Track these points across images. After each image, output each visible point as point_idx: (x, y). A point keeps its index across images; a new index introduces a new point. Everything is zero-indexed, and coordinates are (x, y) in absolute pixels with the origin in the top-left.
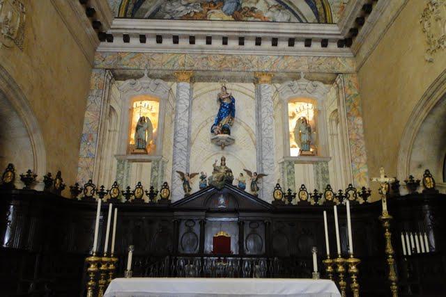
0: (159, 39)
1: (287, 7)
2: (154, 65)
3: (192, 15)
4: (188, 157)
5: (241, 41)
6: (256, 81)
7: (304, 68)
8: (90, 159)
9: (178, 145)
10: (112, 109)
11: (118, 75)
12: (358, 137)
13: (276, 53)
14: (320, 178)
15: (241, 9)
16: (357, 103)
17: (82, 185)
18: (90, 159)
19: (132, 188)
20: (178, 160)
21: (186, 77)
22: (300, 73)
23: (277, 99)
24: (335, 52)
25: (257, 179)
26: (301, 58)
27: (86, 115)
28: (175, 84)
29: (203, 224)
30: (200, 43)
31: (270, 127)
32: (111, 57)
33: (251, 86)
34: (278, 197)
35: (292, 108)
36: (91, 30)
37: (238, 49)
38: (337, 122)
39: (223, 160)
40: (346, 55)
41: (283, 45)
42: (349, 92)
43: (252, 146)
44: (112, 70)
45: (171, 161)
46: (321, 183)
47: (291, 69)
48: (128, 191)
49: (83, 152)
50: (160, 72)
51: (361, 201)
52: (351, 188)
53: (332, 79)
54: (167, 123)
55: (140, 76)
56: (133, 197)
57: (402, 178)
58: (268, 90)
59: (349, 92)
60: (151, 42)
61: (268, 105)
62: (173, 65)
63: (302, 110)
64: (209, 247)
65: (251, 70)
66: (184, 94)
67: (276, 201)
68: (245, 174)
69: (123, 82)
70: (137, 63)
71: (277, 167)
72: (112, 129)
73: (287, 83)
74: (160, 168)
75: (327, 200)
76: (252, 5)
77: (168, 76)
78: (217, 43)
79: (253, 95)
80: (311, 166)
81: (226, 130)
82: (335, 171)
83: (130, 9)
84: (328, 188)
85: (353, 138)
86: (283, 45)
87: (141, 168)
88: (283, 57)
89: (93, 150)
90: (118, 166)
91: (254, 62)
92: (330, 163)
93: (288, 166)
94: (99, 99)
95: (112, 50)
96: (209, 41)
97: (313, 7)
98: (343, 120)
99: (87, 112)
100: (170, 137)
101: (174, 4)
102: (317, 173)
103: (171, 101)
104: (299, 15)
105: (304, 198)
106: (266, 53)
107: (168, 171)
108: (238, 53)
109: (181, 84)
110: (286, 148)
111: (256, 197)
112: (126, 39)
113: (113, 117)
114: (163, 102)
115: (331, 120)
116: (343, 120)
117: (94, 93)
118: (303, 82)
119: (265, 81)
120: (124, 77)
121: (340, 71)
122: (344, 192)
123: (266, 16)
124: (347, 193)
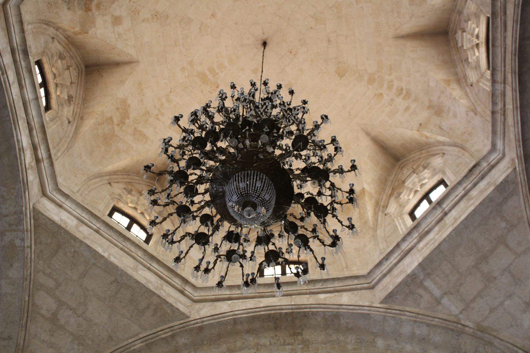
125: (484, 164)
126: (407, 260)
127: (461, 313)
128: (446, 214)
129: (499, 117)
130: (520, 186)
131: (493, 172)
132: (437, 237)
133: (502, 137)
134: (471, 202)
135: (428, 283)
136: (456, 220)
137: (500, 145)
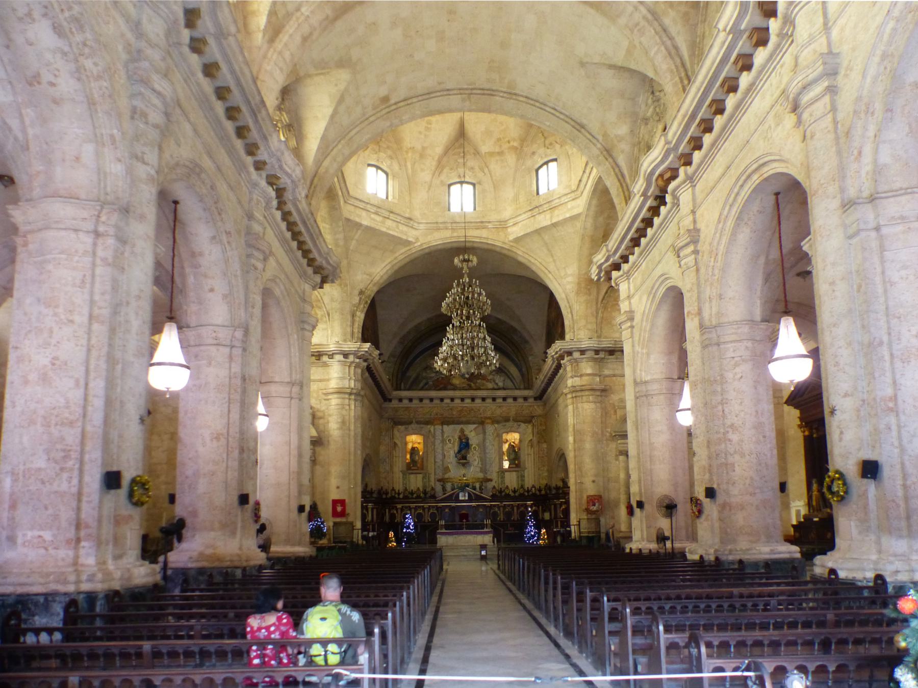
0: (421, 400)
6: (482, 423)
7: (513, 413)
11: (397, 422)
21: (439, 422)
26: (511, 408)
30: (447, 401)
44: (392, 419)
53: (529, 420)
55: (411, 423)
58: (490, 429)
60: (415, 402)
65: (479, 416)
78: (457, 401)
81: (464, 458)
88: (500, 407)
96: (452, 400)
108: (471, 405)
109: (436, 427)
112: (400, 400)
118: (511, 423)
120: (402, 424)
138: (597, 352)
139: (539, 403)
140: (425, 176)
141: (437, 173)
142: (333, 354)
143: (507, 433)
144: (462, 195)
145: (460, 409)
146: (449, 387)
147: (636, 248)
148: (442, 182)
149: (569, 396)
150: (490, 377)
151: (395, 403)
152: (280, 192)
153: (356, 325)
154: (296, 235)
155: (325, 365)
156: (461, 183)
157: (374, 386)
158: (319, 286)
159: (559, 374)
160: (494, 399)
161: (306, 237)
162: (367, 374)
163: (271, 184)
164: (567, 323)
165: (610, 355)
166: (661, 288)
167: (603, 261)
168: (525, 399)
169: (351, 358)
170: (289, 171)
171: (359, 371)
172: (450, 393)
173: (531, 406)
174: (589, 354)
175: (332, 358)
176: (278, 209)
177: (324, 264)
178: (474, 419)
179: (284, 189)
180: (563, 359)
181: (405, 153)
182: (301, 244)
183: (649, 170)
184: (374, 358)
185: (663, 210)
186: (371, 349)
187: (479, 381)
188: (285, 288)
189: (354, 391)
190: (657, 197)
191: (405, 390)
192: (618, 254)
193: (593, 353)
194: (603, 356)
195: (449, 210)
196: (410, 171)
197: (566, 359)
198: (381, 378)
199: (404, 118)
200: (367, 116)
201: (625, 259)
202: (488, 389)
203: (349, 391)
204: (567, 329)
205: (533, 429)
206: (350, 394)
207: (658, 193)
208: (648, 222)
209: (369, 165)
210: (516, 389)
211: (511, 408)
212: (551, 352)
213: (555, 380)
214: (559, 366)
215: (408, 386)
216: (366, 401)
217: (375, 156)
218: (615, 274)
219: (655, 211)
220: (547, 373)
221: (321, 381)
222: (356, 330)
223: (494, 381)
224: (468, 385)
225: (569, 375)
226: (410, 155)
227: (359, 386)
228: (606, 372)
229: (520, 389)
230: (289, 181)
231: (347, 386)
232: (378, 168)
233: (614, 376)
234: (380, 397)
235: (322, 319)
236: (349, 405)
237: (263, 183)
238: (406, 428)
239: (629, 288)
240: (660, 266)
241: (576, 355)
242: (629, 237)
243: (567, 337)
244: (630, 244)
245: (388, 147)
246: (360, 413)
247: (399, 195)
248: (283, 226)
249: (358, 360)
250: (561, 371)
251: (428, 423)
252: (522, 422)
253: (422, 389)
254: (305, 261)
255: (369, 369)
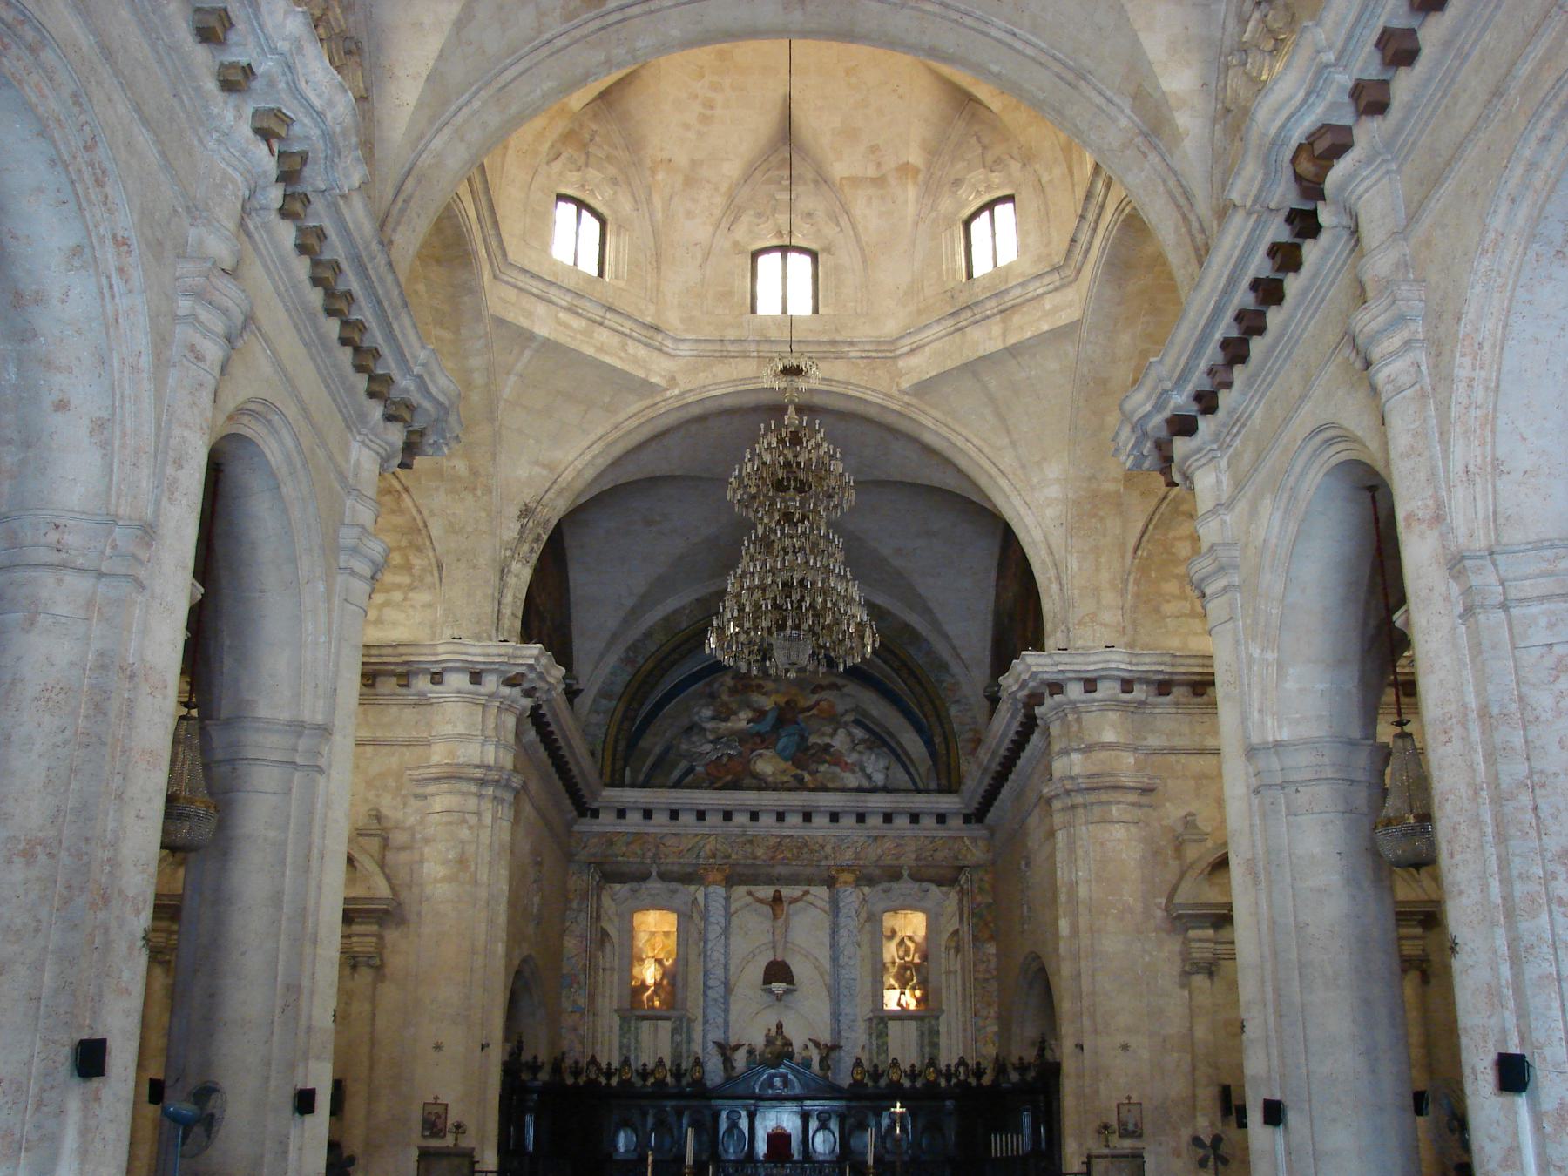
1: (885, 744)
2: (666, 856)
3: (725, 759)
4: (726, 1011)
5: (807, 817)
6: (830, 882)
7: (908, 860)
8: (578, 1015)
9: (710, 992)
10: (605, 934)
11: (611, 874)
12: (987, 976)
13: (866, 833)
14: (926, 1041)
15: (808, 748)
16: (989, 919)
17: (584, 1062)
18: (578, 1015)
19: (651, 1066)
20: (711, 1016)
21: (719, 877)
22: (901, 867)
23: (864, 915)
24: (960, 830)
25: (828, 1054)
26: (905, 843)
27: (566, 943)
28: (702, 888)
29: (752, 1117)
31: (852, 963)
32: (595, 840)
33: (822, 892)
34: (859, 1077)
35: (889, 921)
36: (575, 813)
37: (804, 828)
38: (958, 950)
39: (780, 1026)
40: (976, 834)
41: (875, 821)
42: (979, 898)
43: (825, 993)
45: (700, 1018)
46: (927, 1049)
47: (888, 861)
48: (644, 1070)
49: (567, 1005)
50: (675, 868)
51: (973, 1081)
52: (962, 1062)
53: (949, 877)
54: (692, 957)
55: (644, 877)
56: (651, 1080)
57: (1015, 1059)
58: (851, 897)
59: (979, 898)
60: (660, 818)
61: (849, 923)
62: (698, 857)
63: (913, 924)
64: (761, 1148)
66: (717, 908)
67: (856, 1084)
68: (811, 1045)
69: (617, 887)
70: (639, 852)
71: (861, 1026)
72: (608, 965)
73: (880, 887)
74: (685, 1029)
75: (928, 1081)
76: (827, 740)
77: (690, 874)
79: (827, 907)
80: (913, 1024)
82: (949, 1033)
83: (620, 749)
84: (933, 1062)
85: (980, 976)
86: (875, 821)
87: (656, 1030)
88: (876, 838)
89: (581, 1002)
90: (621, 1028)
91: (828, 849)
92: (943, 1018)
93: (878, 1024)
94: (583, 915)
95: (596, 829)
97: (929, 743)
98: (967, 947)
99: (566, 938)
100: (696, 979)
101: (695, 739)
102: (922, 1034)
103: (695, 915)
104: (905, 758)
105: (895, 1077)
106: (848, 832)
107: (697, 1035)
109: (711, 889)
110: (878, 998)
111: (826, 1078)
112: (621, 813)
113: (608, 947)
114: (684, 919)
115: (948, 948)
116: (967, 947)
117: (574, 905)
119: (845, 883)
120: (622, 878)
121: (966, 863)
122: (953, 1069)
123: (849, 761)
124: (957, 1070)
125: (659, 337)
126: (541, 309)
127: (507, 401)
128: (601, 324)
129: (718, 347)
130: (649, 402)
131: (656, 353)
132: (578, 336)
133: (695, 353)
134: (622, 354)
135: (527, 353)
136: (600, 349)
137: (685, 349)
138: (1127, 685)
139: (977, 830)
140: (696, 229)
141: (724, 225)
142: (444, 669)
143: (895, 910)
144: (785, 277)
145: (773, 841)
146: (748, 781)
147: (1238, 369)
148: (736, 244)
149: (1057, 805)
150: (852, 758)
151: (606, 822)
152: (290, 171)
153: (508, 598)
154: (336, 303)
155: (423, 701)
156: (785, 250)
157: (552, 770)
158: (397, 461)
159: (1029, 748)
160: (861, 818)
161: (364, 311)
162: (532, 734)
163: (265, 134)
164: (1046, 605)
165: (1160, 694)
166: (1310, 476)
167: (1148, 407)
168: (941, 818)
169: (491, 683)
170: (317, 103)
171: (511, 721)
172: (750, 798)
173: (956, 838)
174: (1107, 690)
175: (440, 683)
176: (284, 213)
177: (416, 398)
178: (809, 871)
179: (304, 158)
180: (1041, 704)
181: (648, 173)
182: (352, 334)
183: (1273, 131)
184: (551, 687)
185: (1311, 251)
186: (544, 661)
187: (823, 768)
188: (298, 445)
189: (494, 775)
190: (1293, 217)
191: (633, 786)
192: (1189, 389)
193: (1117, 686)
194: (1142, 696)
195: (753, 310)
196: (659, 216)
197: (1049, 701)
198: (570, 746)
199: (639, 44)
200: (547, 36)
201: (1207, 402)
202: (844, 790)
203: (478, 773)
204: (1048, 627)
205: (961, 901)
206: (483, 782)
207: (1293, 200)
208: (1269, 291)
209: (562, 197)
210: (919, 791)
211: (905, 843)
212: (1008, 682)
213: (1020, 763)
214: (1029, 725)
215: (641, 778)
216: (528, 809)
217: (575, 177)
218: (1180, 446)
219: (1287, 257)
220: (999, 745)
221: (409, 744)
222: (507, 611)
223: (863, 769)
224: (795, 776)
225: (1056, 747)
226: (660, 176)
227: (508, 761)
228: (1154, 741)
229: (927, 791)
230: (315, 133)
231: (477, 761)
232: (581, 205)
233: (1173, 751)
234: (568, 803)
235: (422, 580)
236: (478, 814)
237: (246, 130)
238: (633, 891)
239: (1219, 482)
240: (1307, 407)
241: (1075, 691)
242: (1218, 336)
243: (1050, 642)
244: (1220, 358)
245: (609, 158)
246: (506, 837)
247: (630, 272)
248: (302, 267)
249: (506, 691)
250: (1035, 738)
251: (688, 878)
252: (931, 881)
253: (678, 785)
254: (361, 382)
255: (536, 716)
